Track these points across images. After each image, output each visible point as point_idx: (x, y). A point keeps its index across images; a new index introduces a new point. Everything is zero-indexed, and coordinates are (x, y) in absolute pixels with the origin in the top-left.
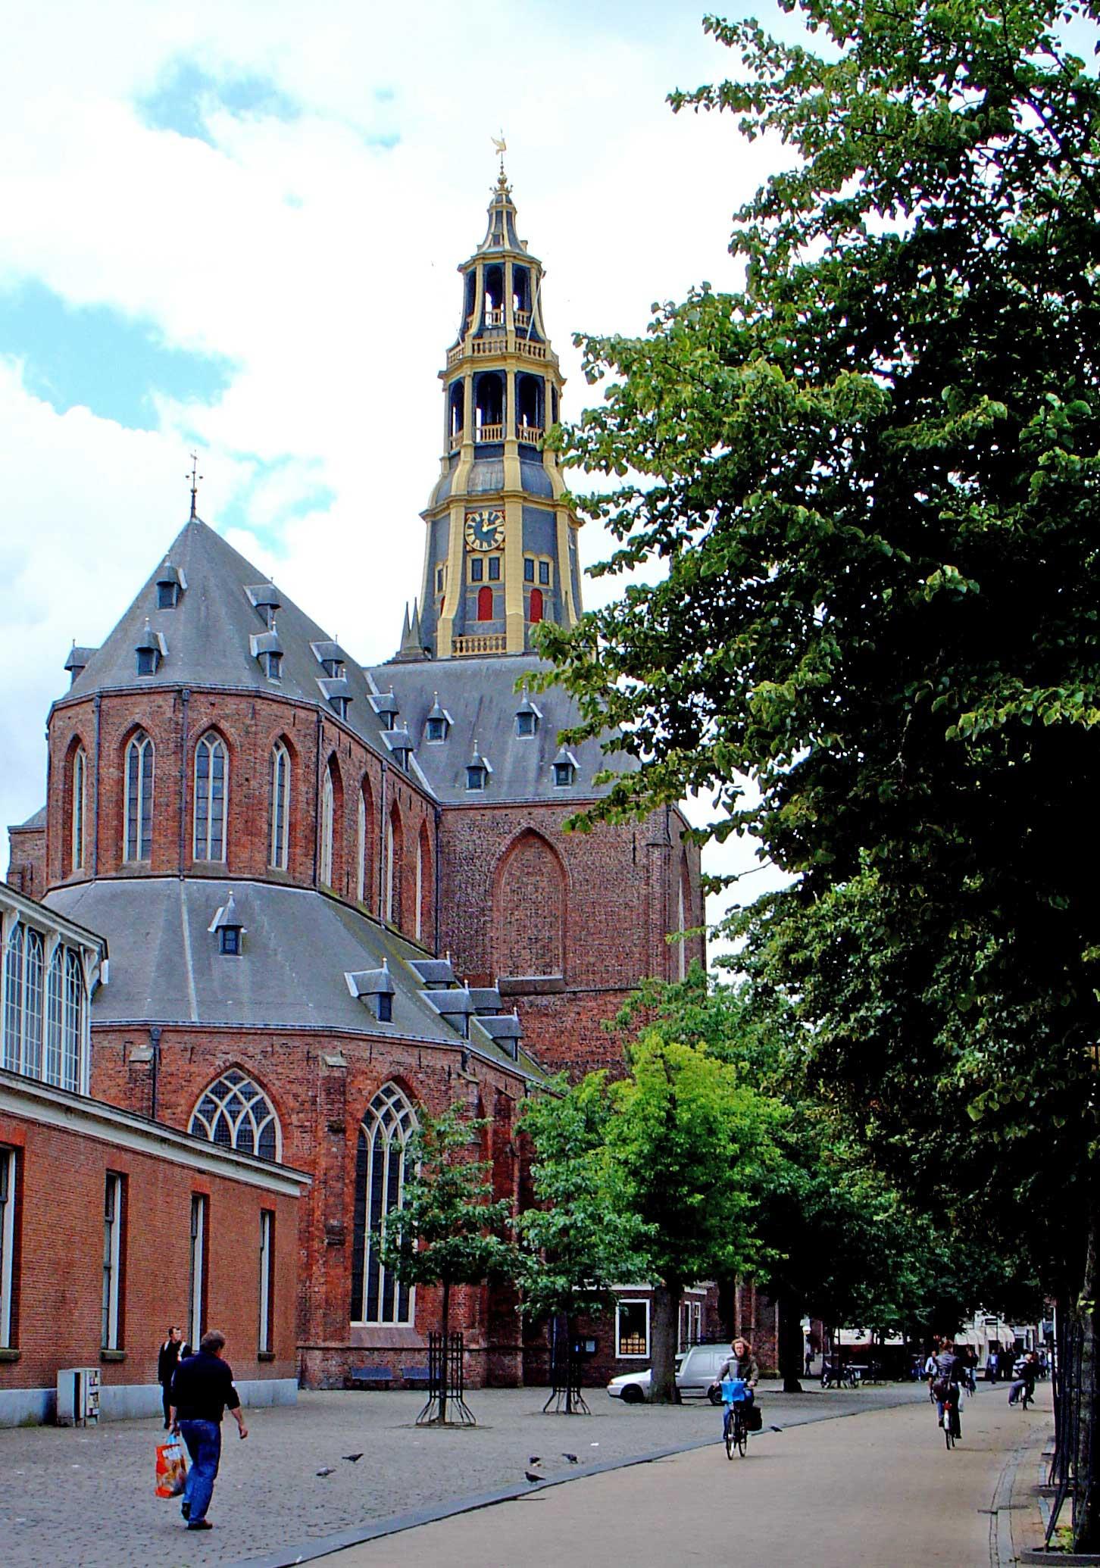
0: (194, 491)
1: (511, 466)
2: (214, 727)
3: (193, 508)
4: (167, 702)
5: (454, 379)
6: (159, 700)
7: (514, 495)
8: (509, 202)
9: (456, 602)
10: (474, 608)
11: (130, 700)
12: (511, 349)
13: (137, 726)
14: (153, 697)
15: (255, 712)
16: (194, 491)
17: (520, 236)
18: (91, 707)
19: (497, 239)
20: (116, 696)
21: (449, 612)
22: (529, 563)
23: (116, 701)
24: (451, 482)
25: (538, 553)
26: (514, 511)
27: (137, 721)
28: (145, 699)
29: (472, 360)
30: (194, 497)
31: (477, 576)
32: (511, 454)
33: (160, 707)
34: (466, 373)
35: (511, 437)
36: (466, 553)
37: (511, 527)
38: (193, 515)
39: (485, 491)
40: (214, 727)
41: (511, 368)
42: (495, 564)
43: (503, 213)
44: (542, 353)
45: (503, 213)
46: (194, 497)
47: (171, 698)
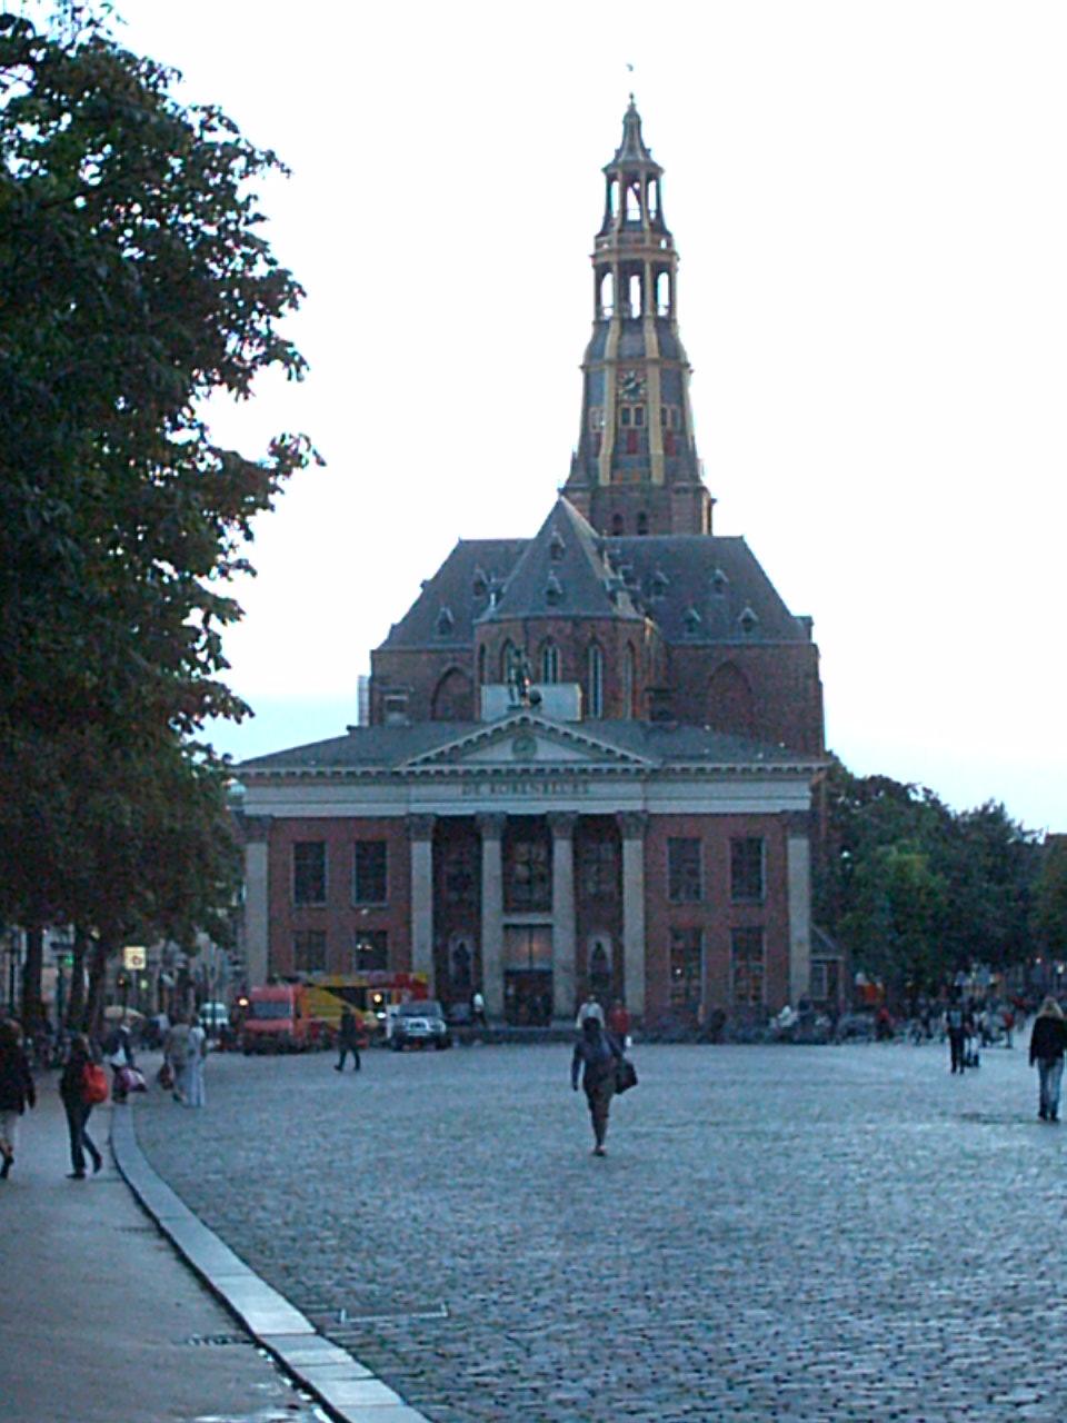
1: (651, 337)
2: (594, 640)
4: (568, 627)
5: (602, 260)
6: (562, 624)
7: (655, 362)
8: (638, 117)
9: (612, 441)
10: (624, 448)
12: (648, 244)
15: (615, 629)
17: (647, 146)
18: (519, 624)
19: (631, 149)
21: (606, 450)
22: (663, 411)
24: (603, 345)
25: (669, 403)
26: (654, 373)
29: (619, 252)
31: (626, 421)
32: (649, 326)
34: (613, 259)
35: (649, 313)
36: (618, 403)
37: (653, 387)
39: (631, 357)
40: (594, 640)
41: (648, 259)
42: (639, 411)
43: (632, 123)
44: (669, 244)
45: (632, 123)
47: (569, 624)
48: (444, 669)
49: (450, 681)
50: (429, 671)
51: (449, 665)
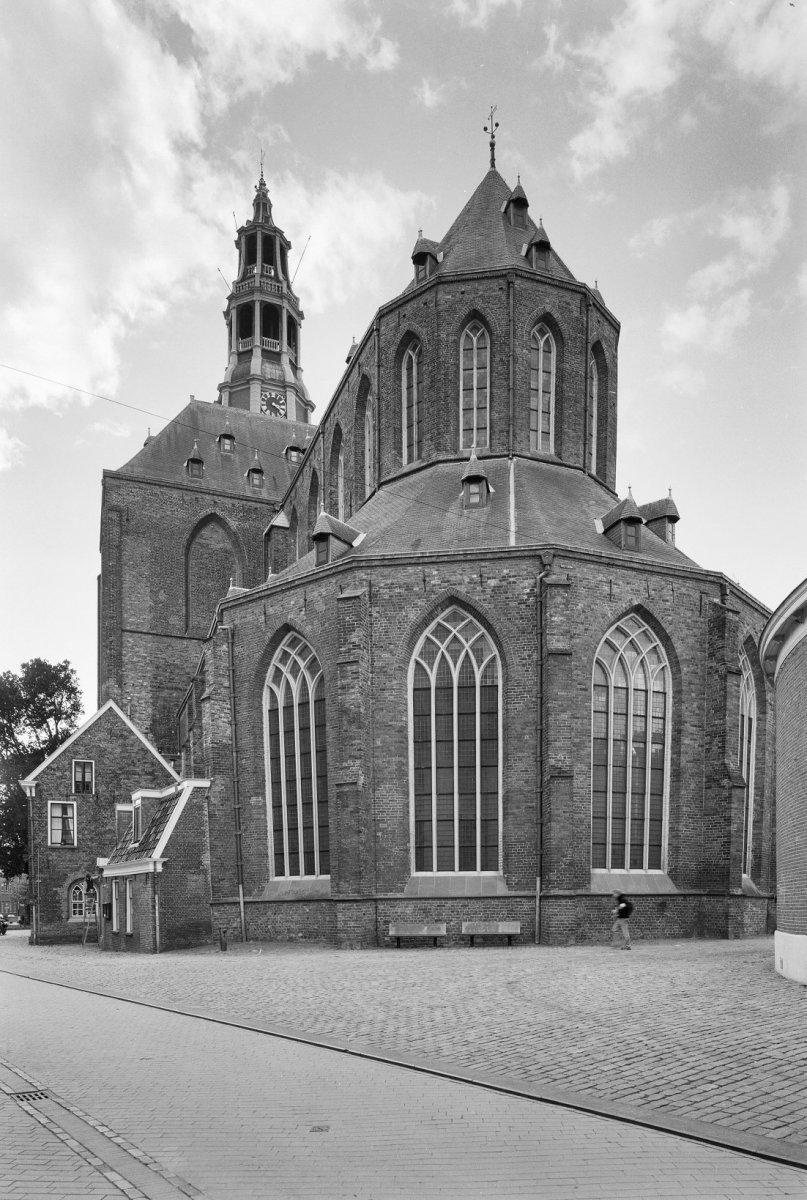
0: (492, 145)
3: (493, 160)
6: (568, 296)
11: (542, 288)
13: (547, 321)
14: (562, 293)
16: (492, 145)
20: (528, 278)
23: (528, 285)
27: (548, 309)
28: (555, 291)
30: (493, 149)
33: (568, 304)
38: (493, 165)
43: (262, 204)
45: (262, 204)
46: (493, 149)
48: (203, 514)
49: (205, 532)
50: (182, 514)
51: (209, 511)
